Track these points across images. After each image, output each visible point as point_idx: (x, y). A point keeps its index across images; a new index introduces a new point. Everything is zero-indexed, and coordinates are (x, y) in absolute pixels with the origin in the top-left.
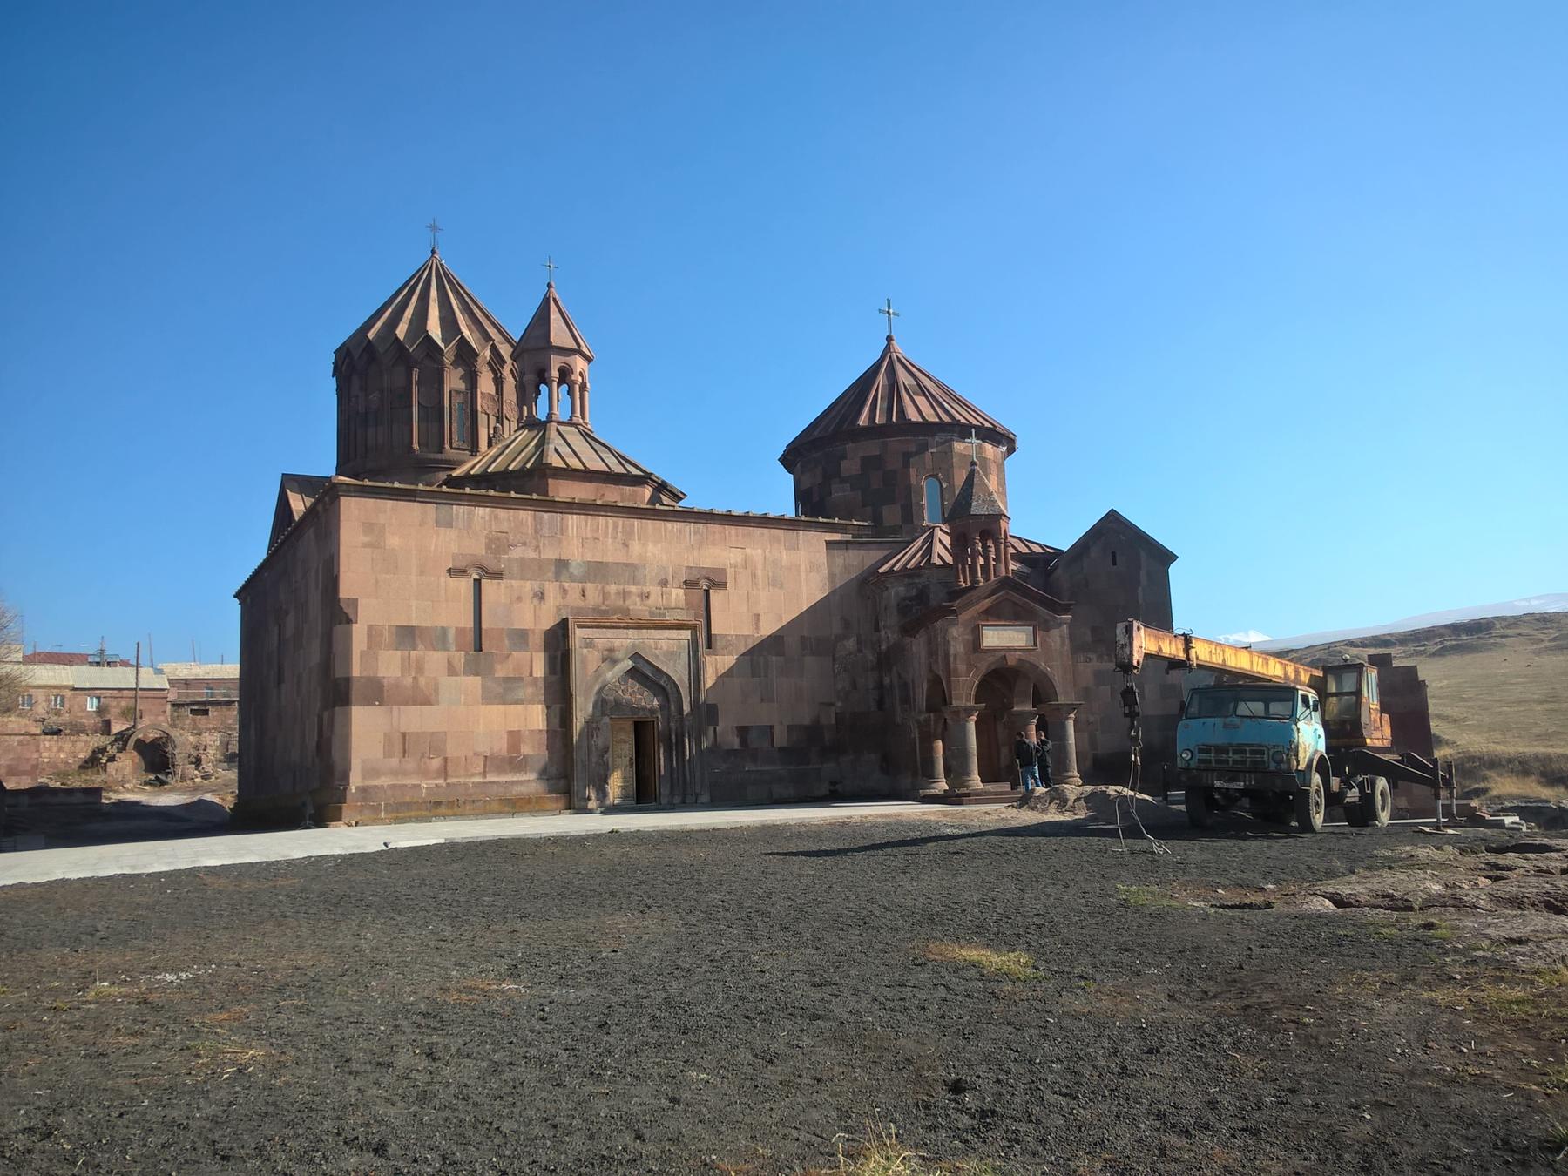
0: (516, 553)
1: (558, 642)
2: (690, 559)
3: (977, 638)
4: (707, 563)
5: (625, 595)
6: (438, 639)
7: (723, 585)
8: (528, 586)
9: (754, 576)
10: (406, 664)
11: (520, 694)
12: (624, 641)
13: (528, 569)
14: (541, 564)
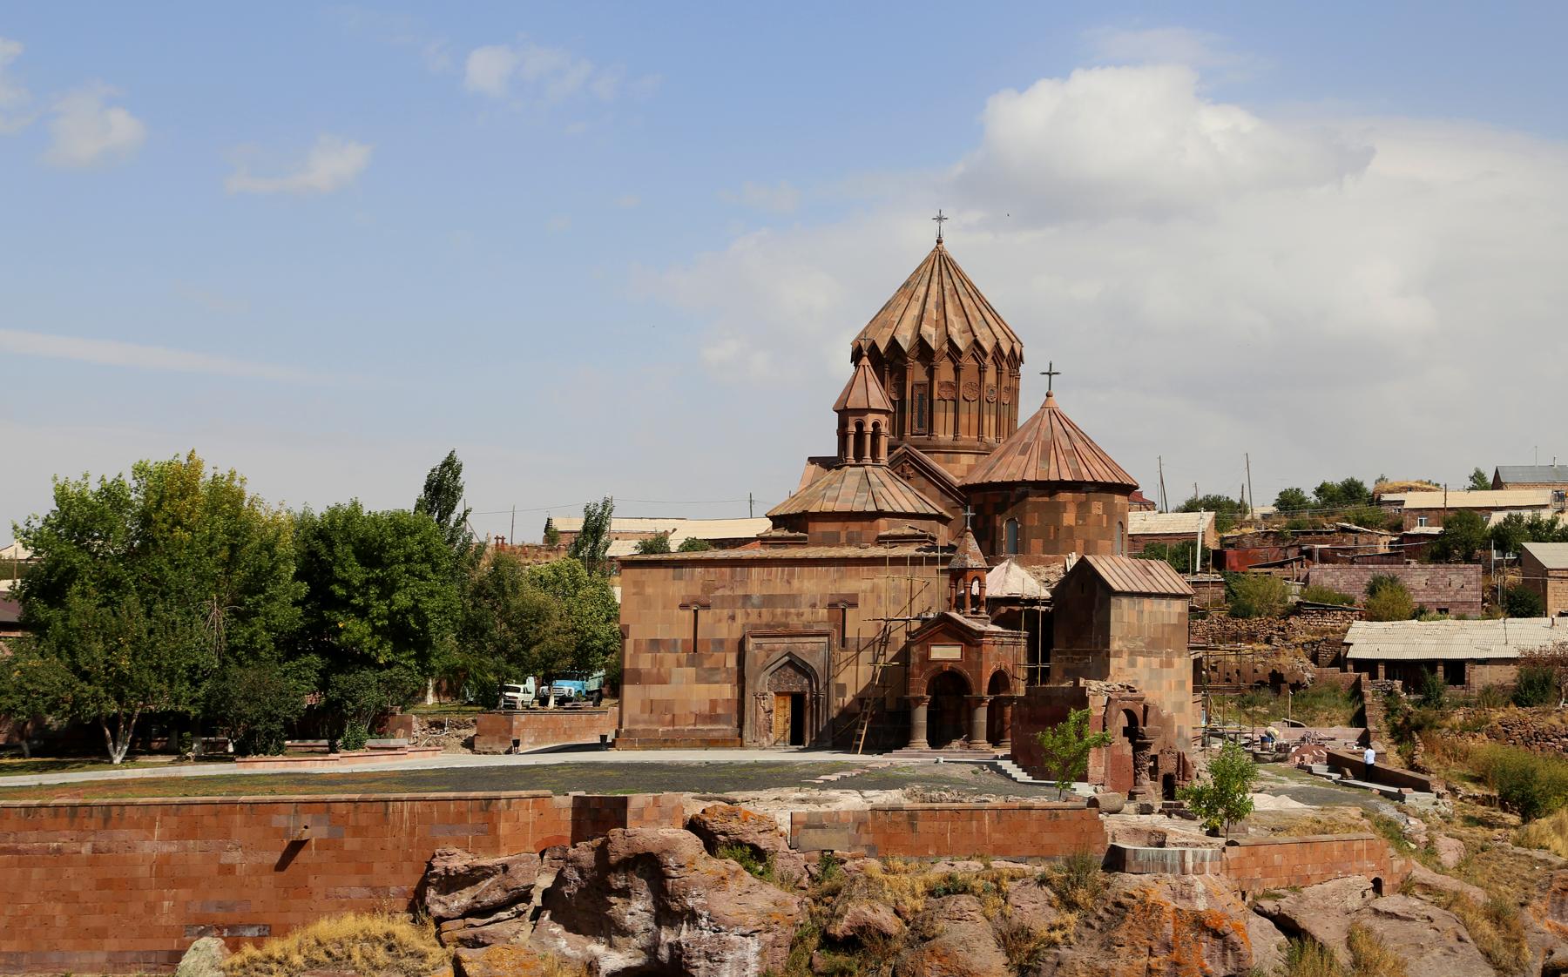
0: (719, 593)
1: (741, 644)
2: (832, 589)
3: (928, 653)
4: (844, 591)
5: (787, 615)
6: (670, 645)
7: (855, 605)
8: (726, 612)
9: (879, 597)
10: (654, 659)
11: (717, 678)
12: (782, 645)
13: (731, 601)
14: (731, 601)
